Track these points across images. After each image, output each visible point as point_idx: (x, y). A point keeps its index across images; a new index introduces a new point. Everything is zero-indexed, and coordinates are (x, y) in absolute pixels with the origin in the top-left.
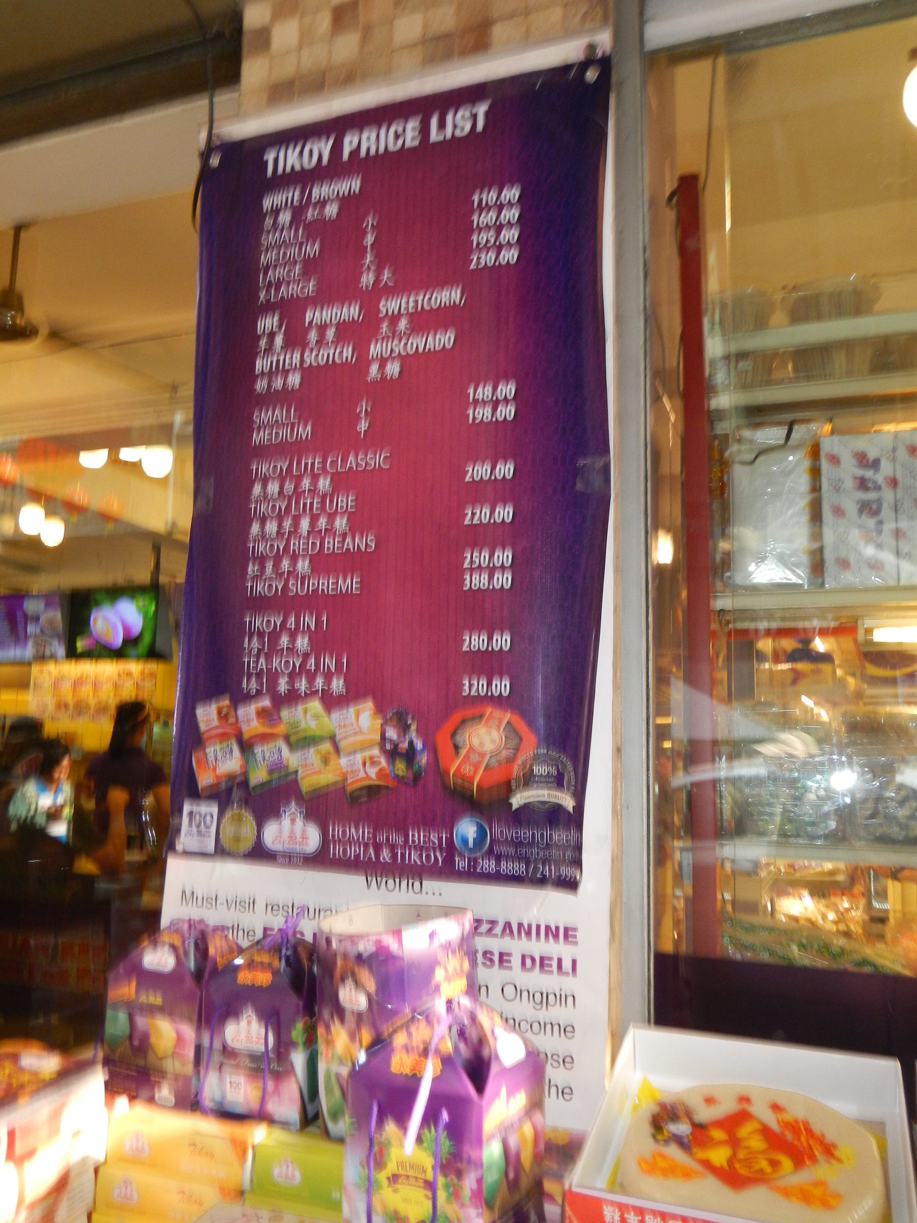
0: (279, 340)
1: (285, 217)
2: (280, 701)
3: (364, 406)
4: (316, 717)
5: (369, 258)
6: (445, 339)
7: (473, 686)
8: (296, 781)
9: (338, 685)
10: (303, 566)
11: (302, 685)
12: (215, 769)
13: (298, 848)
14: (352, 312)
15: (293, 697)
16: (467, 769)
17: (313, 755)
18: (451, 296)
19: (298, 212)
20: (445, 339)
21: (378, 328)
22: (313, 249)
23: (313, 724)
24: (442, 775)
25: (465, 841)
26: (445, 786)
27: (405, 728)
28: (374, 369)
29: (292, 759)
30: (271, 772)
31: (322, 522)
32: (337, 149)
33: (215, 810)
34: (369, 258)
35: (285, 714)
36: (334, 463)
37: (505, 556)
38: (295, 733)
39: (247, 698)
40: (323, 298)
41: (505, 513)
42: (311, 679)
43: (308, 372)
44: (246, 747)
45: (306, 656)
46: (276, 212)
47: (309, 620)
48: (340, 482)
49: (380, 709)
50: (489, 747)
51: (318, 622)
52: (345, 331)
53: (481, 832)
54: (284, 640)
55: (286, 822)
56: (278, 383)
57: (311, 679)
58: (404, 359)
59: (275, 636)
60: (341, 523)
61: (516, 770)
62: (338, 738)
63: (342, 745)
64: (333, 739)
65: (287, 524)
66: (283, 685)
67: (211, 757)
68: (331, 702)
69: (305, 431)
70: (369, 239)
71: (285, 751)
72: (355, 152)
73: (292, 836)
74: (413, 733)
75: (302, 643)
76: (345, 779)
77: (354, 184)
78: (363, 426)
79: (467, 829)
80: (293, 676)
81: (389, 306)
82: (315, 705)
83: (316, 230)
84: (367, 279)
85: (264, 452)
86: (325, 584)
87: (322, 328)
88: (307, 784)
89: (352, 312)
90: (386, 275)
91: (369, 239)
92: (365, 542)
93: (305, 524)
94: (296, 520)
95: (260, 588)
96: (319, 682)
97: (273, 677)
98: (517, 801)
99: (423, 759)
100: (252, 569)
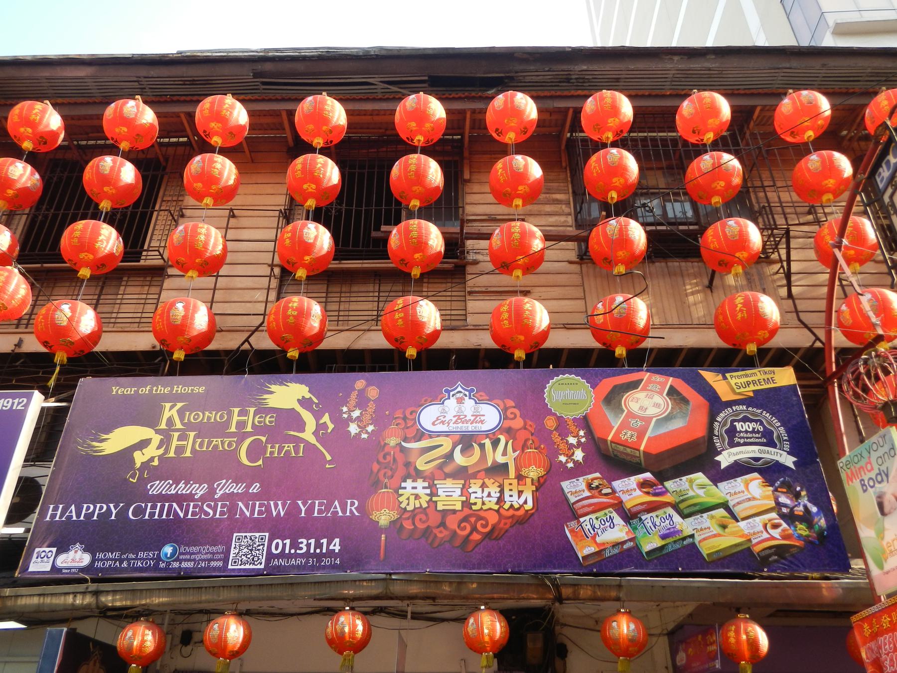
4: (702, 487)
8: (693, 546)
12: (594, 538)
17: (706, 521)
29: (686, 526)
35: (670, 485)
38: (683, 501)
44: (629, 516)
62: (731, 504)
63: (738, 510)
64: (725, 506)
67: (587, 527)
71: (677, 518)
76: (750, 540)
88: (706, 549)
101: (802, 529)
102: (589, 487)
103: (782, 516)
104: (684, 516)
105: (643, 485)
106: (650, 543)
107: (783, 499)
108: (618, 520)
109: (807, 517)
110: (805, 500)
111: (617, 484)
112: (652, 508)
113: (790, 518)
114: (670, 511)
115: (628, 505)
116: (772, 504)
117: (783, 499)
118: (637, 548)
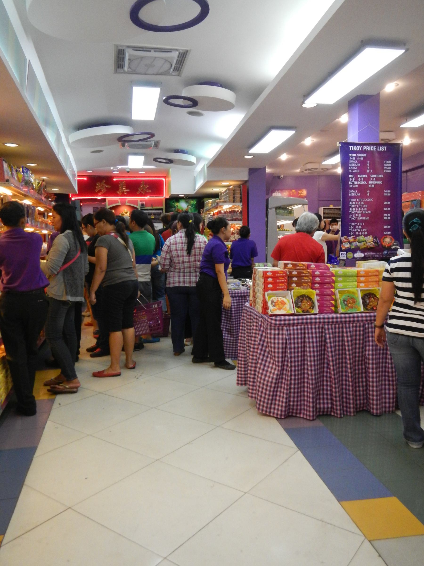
0: (354, 179)
1: (354, 158)
2: (357, 236)
3: (368, 191)
5: (368, 168)
6: (381, 182)
7: (386, 233)
9: (366, 233)
10: (360, 215)
11: (360, 233)
13: (360, 257)
14: (366, 176)
15: (359, 235)
16: (385, 244)
17: (362, 244)
18: (381, 176)
19: (356, 158)
20: (381, 182)
21: (370, 179)
22: (359, 165)
23: (362, 239)
24: (382, 245)
25: (385, 254)
26: (383, 247)
27: (376, 239)
28: (370, 185)
29: (359, 244)
30: (355, 246)
31: (362, 209)
32: (362, 148)
33: (346, 253)
34: (368, 168)
35: (357, 238)
36: (364, 200)
37: (389, 215)
39: (351, 236)
40: (360, 174)
41: (389, 209)
42: (362, 233)
43: (359, 185)
44: (350, 243)
45: (361, 229)
46: (352, 157)
47: (361, 224)
48: (366, 203)
49: (373, 237)
50: (388, 241)
51: (363, 224)
52: (365, 179)
53: (387, 252)
54: (357, 227)
55: (358, 253)
56: (354, 186)
57: (362, 233)
58: (375, 185)
59: (355, 226)
60: (365, 209)
61: (392, 244)
63: (367, 242)
65: (357, 209)
66: (357, 233)
68: (365, 236)
69: (359, 195)
70: (368, 165)
71: (358, 243)
72: (365, 149)
73: (359, 255)
74: (378, 240)
75: (360, 227)
77: (365, 155)
78: (368, 194)
79: (386, 252)
80: (359, 232)
81: (372, 176)
82: (363, 236)
83: (359, 162)
84: (368, 171)
85: (351, 197)
86: (363, 218)
87: (361, 178)
89: (366, 176)
90: (371, 171)
91: (368, 165)
92: (369, 212)
93: (360, 209)
94: (358, 209)
95: (352, 219)
96: (363, 233)
97: (355, 232)
98: (392, 248)
99: (379, 243)
100: (350, 216)
101: (376, 245)
102: (345, 238)
103: (374, 242)
104: (359, 243)
105: (353, 238)
106: (353, 247)
107: (375, 240)
108: (348, 244)
109: (377, 243)
110: (378, 240)
111: (349, 238)
112: (354, 242)
113: (375, 243)
114: (357, 242)
115: (350, 241)
116: (372, 240)
117: (375, 240)
118: (351, 248)
